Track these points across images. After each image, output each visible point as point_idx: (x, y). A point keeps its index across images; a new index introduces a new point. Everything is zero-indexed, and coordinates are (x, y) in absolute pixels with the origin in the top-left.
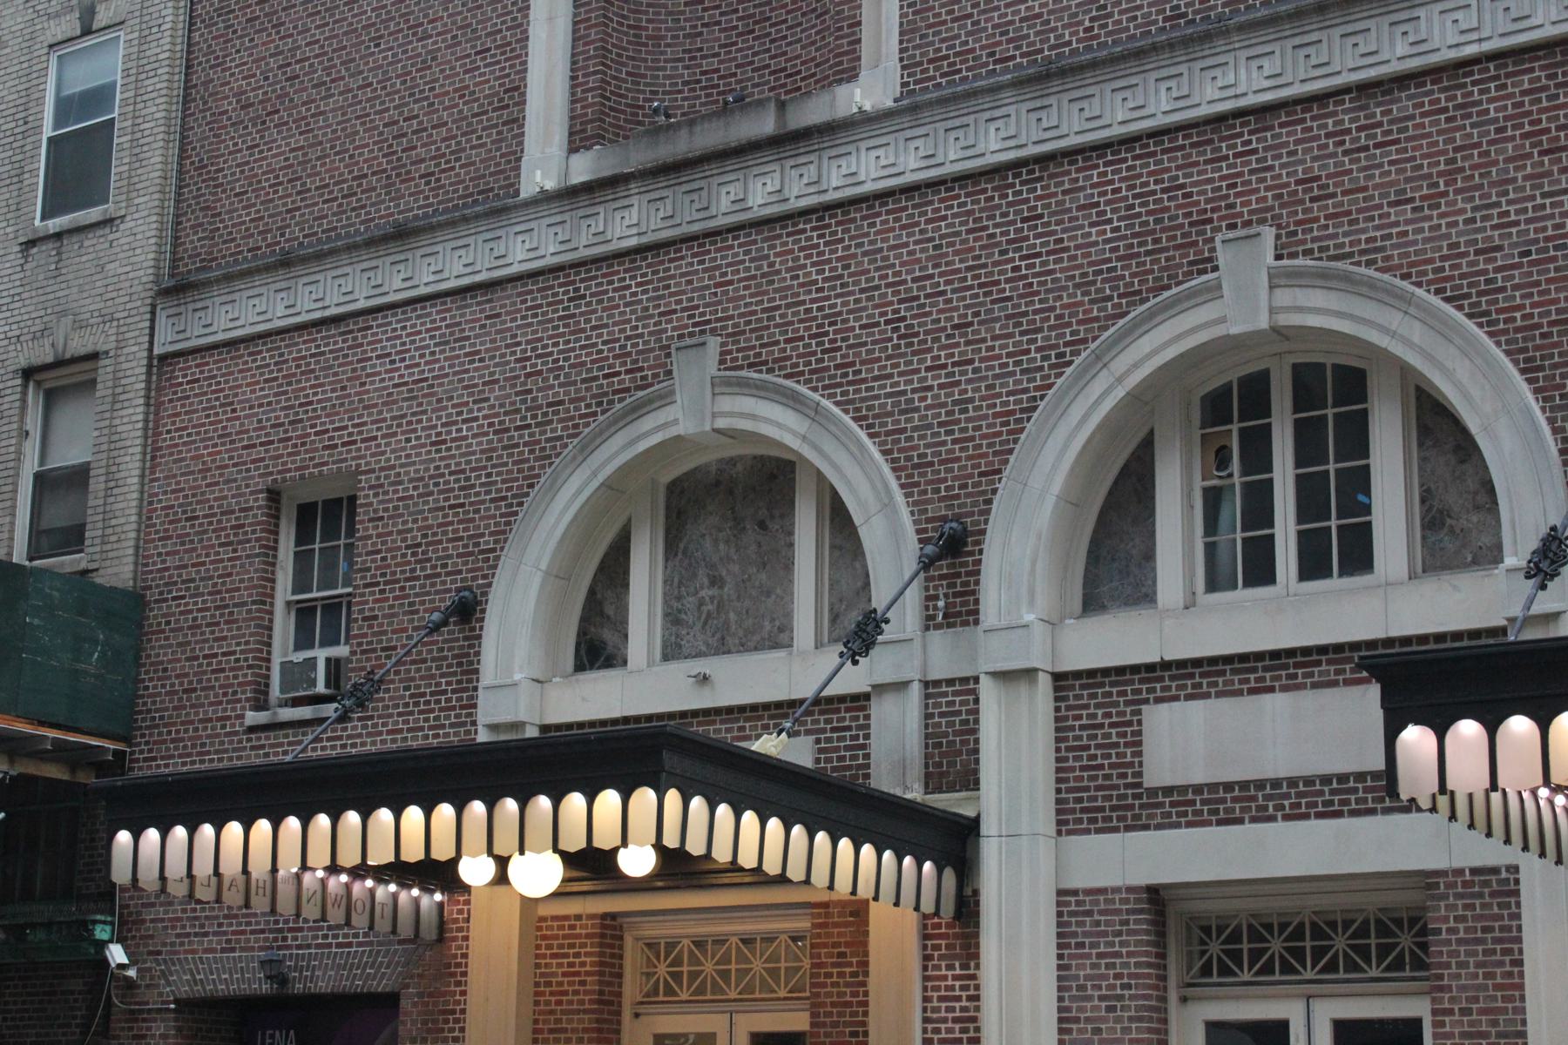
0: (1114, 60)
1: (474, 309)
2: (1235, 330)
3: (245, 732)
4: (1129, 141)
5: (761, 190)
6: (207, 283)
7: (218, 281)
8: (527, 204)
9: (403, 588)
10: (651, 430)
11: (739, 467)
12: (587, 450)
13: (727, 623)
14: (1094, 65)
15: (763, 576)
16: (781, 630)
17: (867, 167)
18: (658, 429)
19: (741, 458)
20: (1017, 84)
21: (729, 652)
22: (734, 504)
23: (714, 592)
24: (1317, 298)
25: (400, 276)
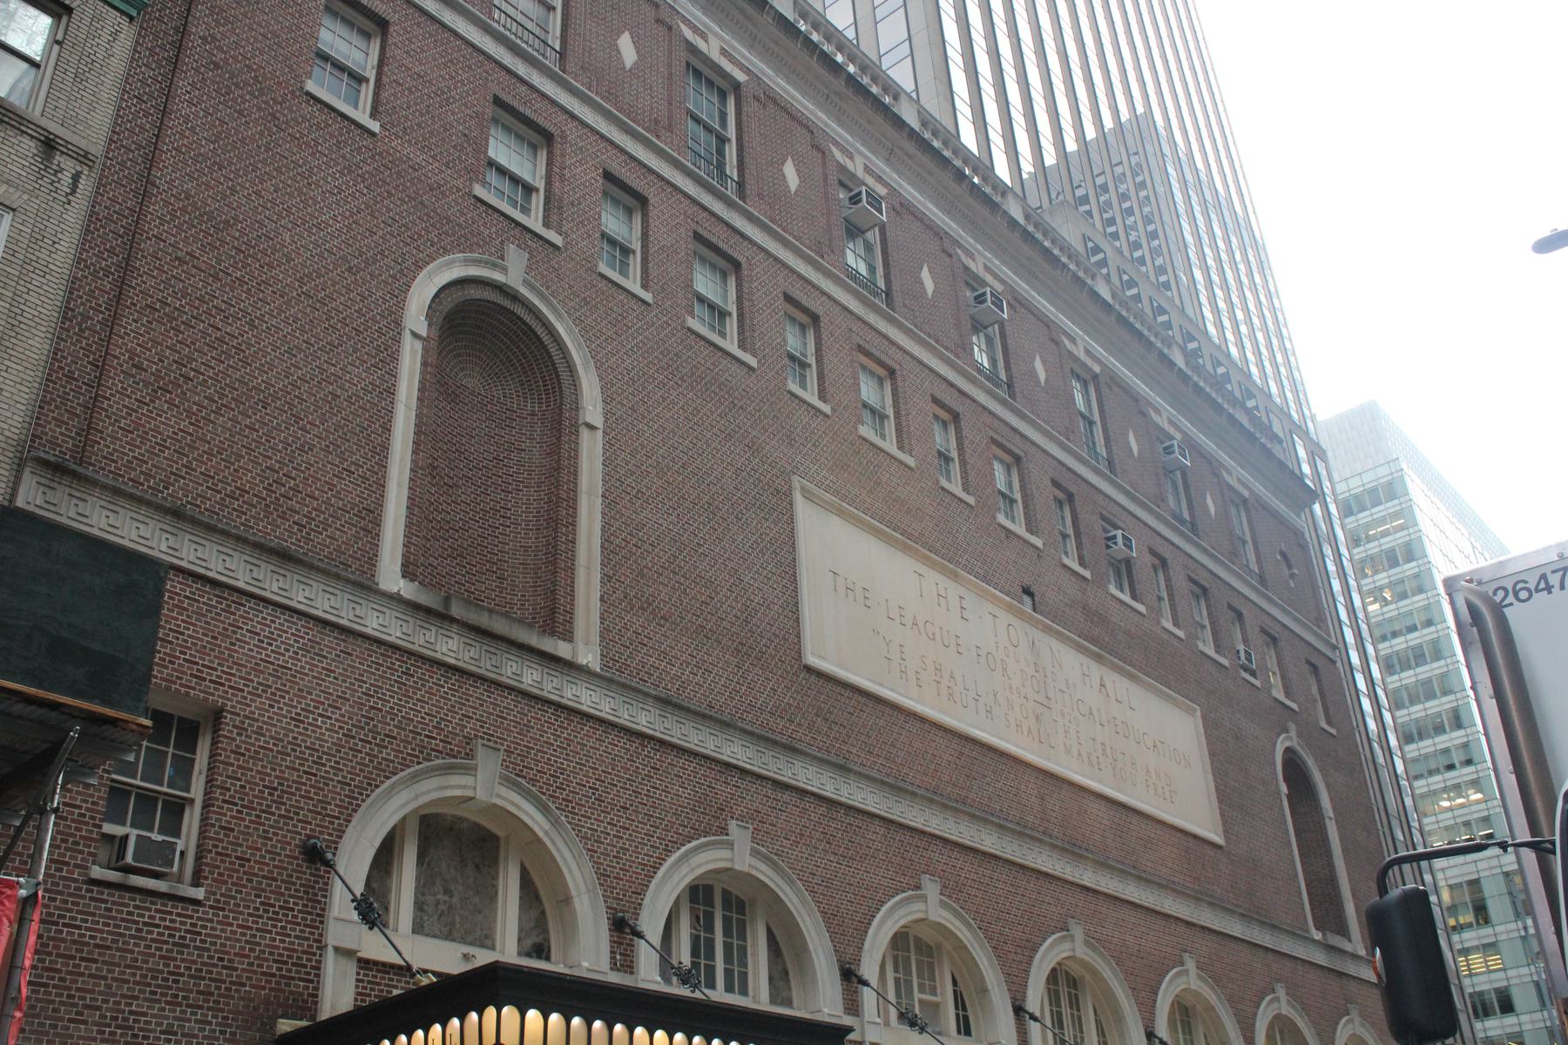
0: (697, 714)
1: (329, 640)
2: (737, 867)
3: (84, 882)
4: (696, 754)
5: (531, 677)
6: (94, 483)
7: (105, 487)
8: (385, 595)
9: (258, 816)
10: (455, 786)
11: (465, 825)
12: (415, 778)
13: (453, 923)
14: (688, 710)
15: (477, 900)
16: (487, 937)
17: (586, 697)
18: (460, 787)
19: (466, 820)
20: (658, 699)
21: (454, 940)
22: (460, 849)
23: (446, 898)
24: (763, 867)
25: (273, 583)
